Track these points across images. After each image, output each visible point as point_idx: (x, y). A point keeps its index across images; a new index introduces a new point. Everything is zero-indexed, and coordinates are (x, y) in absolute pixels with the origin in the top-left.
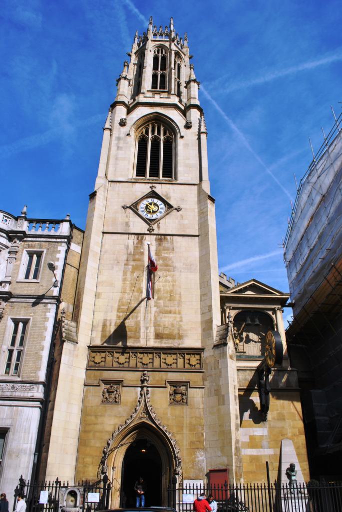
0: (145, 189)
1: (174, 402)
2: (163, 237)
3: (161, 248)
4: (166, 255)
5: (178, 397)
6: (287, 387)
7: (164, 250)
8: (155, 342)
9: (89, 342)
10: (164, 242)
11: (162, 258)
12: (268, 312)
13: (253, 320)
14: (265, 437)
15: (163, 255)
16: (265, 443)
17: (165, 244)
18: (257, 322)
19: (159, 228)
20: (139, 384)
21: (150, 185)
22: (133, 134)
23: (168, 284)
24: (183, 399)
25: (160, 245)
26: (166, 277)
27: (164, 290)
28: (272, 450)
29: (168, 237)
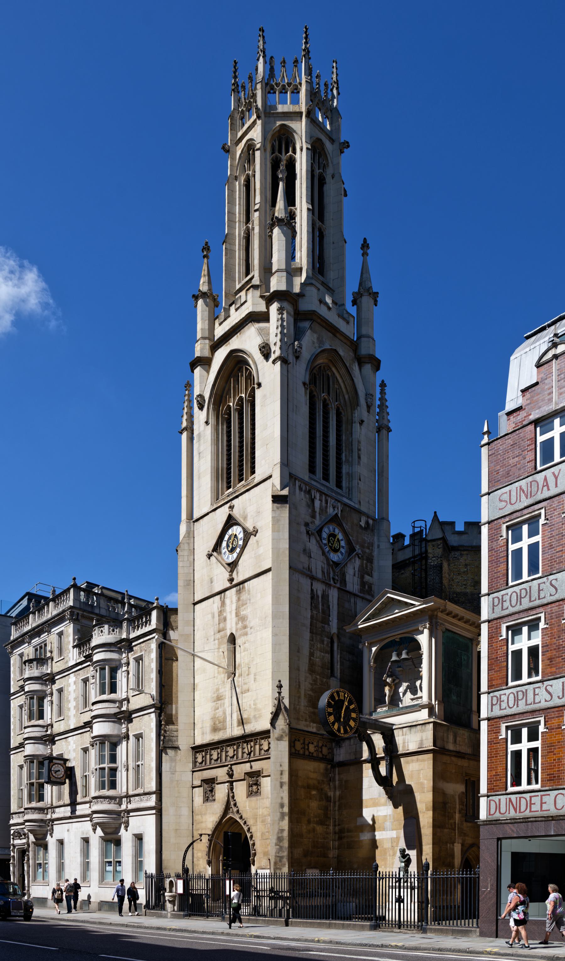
0: (222, 515)
1: (250, 794)
2: (241, 586)
3: (240, 602)
4: (244, 612)
5: (255, 787)
6: (419, 748)
7: (243, 605)
8: (238, 730)
9: (192, 742)
10: (242, 595)
11: (241, 618)
12: (373, 651)
13: (399, 655)
14: (388, 817)
15: (242, 613)
16: (388, 824)
17: (244, 596)
18: (404, 656)
19: (237, 573)
20: (227, 778)
21: (228, 505)
22: (212, 420)
23: (246, 652)
24: (258, 789)
25: (239, 599)
26: (245, 643)
27: (243, 663)
28: (395, 832)
29: (246, 584)
